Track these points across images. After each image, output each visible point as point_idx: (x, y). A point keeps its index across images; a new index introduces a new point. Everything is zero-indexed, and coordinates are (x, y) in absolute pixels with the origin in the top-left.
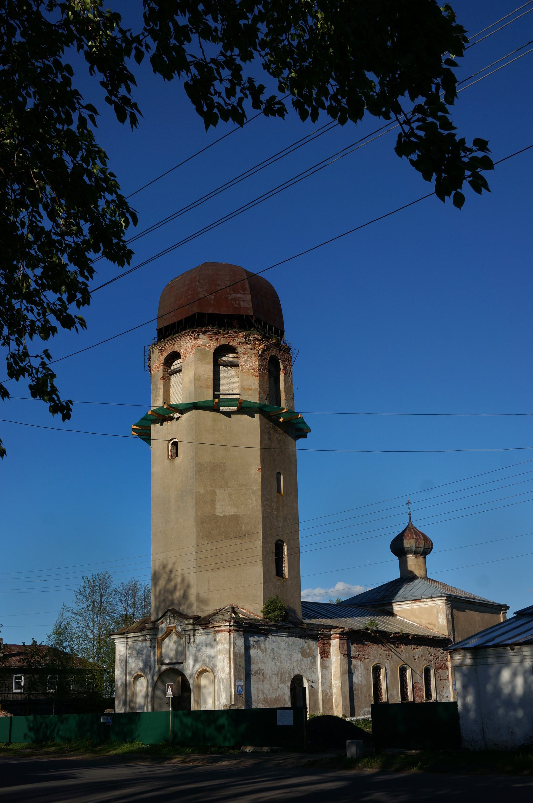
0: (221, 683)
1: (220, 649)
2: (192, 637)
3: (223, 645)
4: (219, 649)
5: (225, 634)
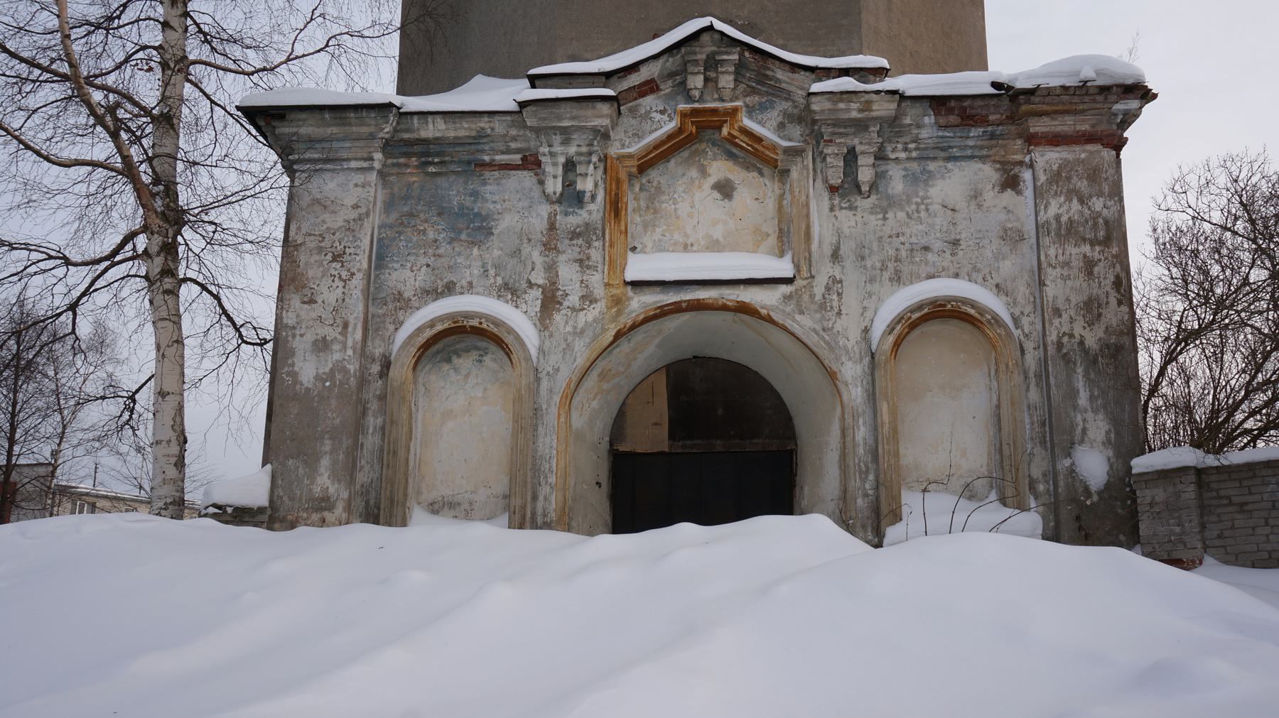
0: (1080, 370)
1: (1064, 219)
2: (865, 161)
3: (1081, 201)
4: (1058, 218)
5: (1091, 153)
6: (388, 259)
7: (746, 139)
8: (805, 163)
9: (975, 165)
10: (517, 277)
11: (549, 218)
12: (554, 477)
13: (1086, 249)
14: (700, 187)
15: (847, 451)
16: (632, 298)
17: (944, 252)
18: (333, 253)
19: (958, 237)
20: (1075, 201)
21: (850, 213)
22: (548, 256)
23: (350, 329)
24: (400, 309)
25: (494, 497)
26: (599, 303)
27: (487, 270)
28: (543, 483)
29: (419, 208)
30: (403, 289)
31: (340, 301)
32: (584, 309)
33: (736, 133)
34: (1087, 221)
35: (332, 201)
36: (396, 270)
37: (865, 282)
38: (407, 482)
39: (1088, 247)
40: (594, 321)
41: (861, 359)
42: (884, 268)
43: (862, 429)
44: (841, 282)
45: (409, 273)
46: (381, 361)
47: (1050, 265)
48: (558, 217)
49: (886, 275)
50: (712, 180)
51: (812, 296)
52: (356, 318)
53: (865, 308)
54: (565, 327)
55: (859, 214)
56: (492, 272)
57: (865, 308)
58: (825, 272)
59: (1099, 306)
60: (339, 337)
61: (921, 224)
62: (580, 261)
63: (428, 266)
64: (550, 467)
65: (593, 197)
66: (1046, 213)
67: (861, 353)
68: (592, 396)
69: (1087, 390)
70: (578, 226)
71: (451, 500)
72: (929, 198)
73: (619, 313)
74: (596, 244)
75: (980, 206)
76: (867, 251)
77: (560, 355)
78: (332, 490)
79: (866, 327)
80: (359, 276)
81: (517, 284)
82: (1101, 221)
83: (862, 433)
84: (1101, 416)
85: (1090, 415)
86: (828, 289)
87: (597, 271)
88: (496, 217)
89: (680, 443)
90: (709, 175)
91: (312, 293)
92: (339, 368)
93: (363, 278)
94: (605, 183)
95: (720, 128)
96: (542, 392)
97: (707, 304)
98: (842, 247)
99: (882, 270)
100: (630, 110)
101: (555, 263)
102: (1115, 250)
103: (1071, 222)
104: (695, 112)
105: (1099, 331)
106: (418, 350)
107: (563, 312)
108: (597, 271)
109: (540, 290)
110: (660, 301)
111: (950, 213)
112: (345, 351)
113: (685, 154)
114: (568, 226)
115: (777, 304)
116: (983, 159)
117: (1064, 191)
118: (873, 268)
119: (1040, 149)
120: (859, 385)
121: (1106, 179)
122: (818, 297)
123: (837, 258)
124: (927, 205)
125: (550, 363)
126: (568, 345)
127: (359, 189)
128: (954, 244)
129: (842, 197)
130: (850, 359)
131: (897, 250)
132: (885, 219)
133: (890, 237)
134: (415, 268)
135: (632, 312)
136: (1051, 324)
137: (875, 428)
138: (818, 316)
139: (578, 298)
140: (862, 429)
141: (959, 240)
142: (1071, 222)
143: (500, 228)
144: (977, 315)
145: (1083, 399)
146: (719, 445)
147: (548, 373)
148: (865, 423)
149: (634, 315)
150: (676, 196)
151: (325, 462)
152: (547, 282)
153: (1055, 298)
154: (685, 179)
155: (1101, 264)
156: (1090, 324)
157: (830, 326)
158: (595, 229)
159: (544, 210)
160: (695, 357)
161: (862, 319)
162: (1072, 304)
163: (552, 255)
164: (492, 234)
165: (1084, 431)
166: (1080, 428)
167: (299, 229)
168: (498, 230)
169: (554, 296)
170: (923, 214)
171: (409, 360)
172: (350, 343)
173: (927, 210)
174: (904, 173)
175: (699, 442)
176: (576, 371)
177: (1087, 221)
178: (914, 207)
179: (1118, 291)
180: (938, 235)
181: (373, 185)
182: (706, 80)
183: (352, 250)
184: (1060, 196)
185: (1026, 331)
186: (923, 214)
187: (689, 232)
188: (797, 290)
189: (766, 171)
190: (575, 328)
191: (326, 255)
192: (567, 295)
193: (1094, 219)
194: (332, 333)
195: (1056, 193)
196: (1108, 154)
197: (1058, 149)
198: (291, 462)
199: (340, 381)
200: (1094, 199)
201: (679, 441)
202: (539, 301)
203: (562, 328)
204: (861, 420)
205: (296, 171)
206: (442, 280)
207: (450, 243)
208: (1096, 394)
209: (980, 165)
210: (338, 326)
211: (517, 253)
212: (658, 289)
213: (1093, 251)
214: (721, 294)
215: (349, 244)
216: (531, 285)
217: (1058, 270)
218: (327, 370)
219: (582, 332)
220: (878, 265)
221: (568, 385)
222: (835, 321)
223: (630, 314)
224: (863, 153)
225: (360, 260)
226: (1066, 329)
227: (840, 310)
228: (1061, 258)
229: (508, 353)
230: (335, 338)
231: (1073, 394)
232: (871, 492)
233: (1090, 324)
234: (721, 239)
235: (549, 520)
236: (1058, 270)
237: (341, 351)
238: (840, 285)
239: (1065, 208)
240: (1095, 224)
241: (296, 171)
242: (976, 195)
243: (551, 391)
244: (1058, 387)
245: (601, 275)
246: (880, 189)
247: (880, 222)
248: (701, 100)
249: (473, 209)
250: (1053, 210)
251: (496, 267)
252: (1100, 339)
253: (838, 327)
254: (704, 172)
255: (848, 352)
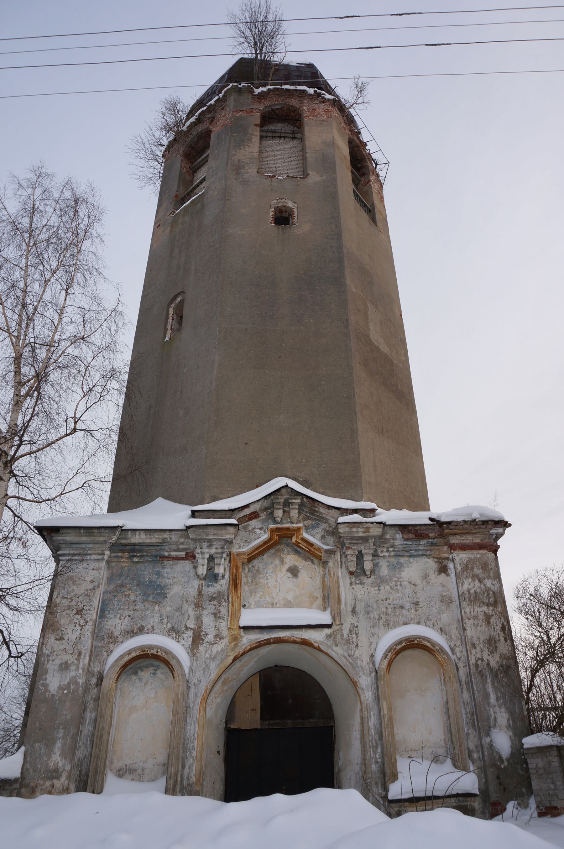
0: (489, 681)
1: (472, 591)
3: (480, 581)
4: (469, 590)
5: (482, 555)
6: (107, 612)
7: (305, 544)
8: (336, 558)
9: (425, 560)
10: (179, 623)
11: (199, 588)
12: (195, 751)
13: (485, 608)
14: (280, 570)
15: (365, 732)
16: (243, 637)
17: (411, 609)
18: (77, 609)
19: (418, 601)
20: (477, 581)
21: (361, 586)
22: (197, 611)
23: (82, 656)
24: (111, 643)
25: (157, 765)
26: (225, 640)
27: (163, 619)
28: (188, 757)
29: (127, 581)
30: (114, 630)
31: (78, 639)
32: (216, 643)
33: (299, 541)
34: (484, 593)
35: (79, 578)
36: (111, 619)
37: (371, 627)
38: (106, 757)
39: (486, 607)
40: (222, 650)
41: (370, 674)
42: (380, 619)
43: (373, 718)
44: (357, 627)
45: (118, 621)
46: (98, 676)
47: (467, 618)
48: (203, 588)
49: (382, 623)
50: (287, 566)
51: (342, 635)
52: (86, 649)
53: (371, 642)
54: (205, 654)
55: (366, 587)
56: (165, 620)
57: (371, 642)
58: (348, 621)
59: (495, 642)
60: (76, 662)
61: (398, 593)
62: (215, 614)
63: (129, 616)
64: (193, 746)
65: (223, 577)
66: (462, 588)
67: (370, 670)
68: (218, 695)
69: (494, 693)
70: (214, 593)
71: (131, 767)
72: (401, 578)
73: (236, 646)
74: (224, 604)
75: (428, 583)
76: (371, 609)
77: (202, 672)
78: (60, 764)
79: (372, 654)
80: (90, 623)
81: (179, 628)
82: (491, 592)
83: (373, 721)
84: (503, 710)
85: (497, 709)
86: (351, 631)
87: (224, 620)
88: (169, 587)
89: (267, 722)
90: (285, 563)
91: (62, 634)
92: (73, 681)
93: (93, 625)
94: (230, 568)
95: (291, 538)
96: (190, 696)
97: (285, 640)
98: (357, 606)
99: (379, 620)
100: (244, 528)
101: (201, 615)
102: (500, 609)
103: (476, 593)
104: (278, 529)
105: (497, 657)
106: (120, 669)
107: (204, 645)
108: (224, 620)
109: (192, 631)
110: (258, 639)
111: (413, 586)
112: (78, 670)
113: (272, 551)
114: (209, 593)
115: (323, 640)
116: (428, 556)
117: (471, 575)
118: (374, 618)
119: (456, 552)
120: (370, 689)
121: (491, 569)
122: (345, 636)
123: (355, 613)
124: (401, 582)
125: (196, 677)
126: (206, 666)
127: (95, 571)
128: (416, 604)
129: (356, 577)
130: (364, 674)
131: (386, 608)
132: (379, 590)
133: (382, 600)
134: (122, 618)
135: (243, 645)
136: (471, 653)
137: (380, 718)
138: (346, 647)
139: (212, 637)
140: (373, 718)
141: (418, 602)
142: (476, 593)
143: (171, 593)
144: (431, 647)
145: (493, 700)
146: (290, 723)
147: (194, 684)
148: (374, 715)
149: (244, 647)
150: (267, 575)
151: (58, 745)
152: (196, 626)
153: (472, 637)
154: (272, 565)
155: (494, 617)
156: (492, 652)
157: (352, 653)
158: (224, 595)
159: (196, 583)
160: (276, 666)
161: (370, 649)
162: (481, 641)
163: (199, 610)
164: (167, 597)
165: (495, 719)
166: (493, 717)
167: (59, 594)
168: (170, 595)
169: (200, 635)
170: (399, 587)
171: (114, 676)
172: (81, 665)
173: (401, 585)
174: (388, 564)
175: (278, 721)
176: (210, 682)
177: (484, 593)
178: (394, 583)
179: (504, 633)
180: (408, 599)
181: (103, 569)
182: (284, 512)
183: (87, 608)
184: (469, 578)
185: (458, 656)
186: (399, 587)
187: (274, 596)
188: (333, 632)
189: (316, 561)
190: (211, 655)
191: (72, 610)
192: (207, 634)
193: (487, 591)
194: (71, 659)
195: (467, 576)
196: (491, 555)
197: (465, 552)
198: (37, 745)
199: (73, 690)
200: (486, 580)
201: (266, 721)
202: (191, 638)
203: (204, 655)
204: (372, 713)
205: (60, 560)
206: (137, 625)
207: (143, 603)
208: (499, 695)
209: (427, 560)
210: (75, 654)
211: (179, 609)
212: (258, 631)
213: (489, 610)
214: (292, 634)
215: (86, 604)
216: (187, 628)
217: (472, 621)
218: (66, 683)
219: (215, 658)
220: (377, 617)
221: (206, 690)
222: (355, 651)
223: (241, 646)
224: (366, 554)
225: (91, 614)
226: (479, 656)
227: (358, 644)
228: (473, 614)
229: (172, 670)
230: (73, 662)
231: (486, 696)
232: (379, 760)
233: (492, 652)
234: (292, 600)
235: (191, 783)
236: (472, 621)
237: (75, 670)
238: (357, 629)
239: (472, 585)
240: (488, 594)
241: (60, 560)
242: (426, 577)
243: (196, 695)
244: (478, 691)
245: (226, 622)
246: (376, 573)
247: (377, 592)
248: (281, 522)
249: (156, 582)
250: (466, 586)
251: (168, 617)
252: (498, 662)
253: (357, 654)
254: (282, 562)
255: (363, 669)
